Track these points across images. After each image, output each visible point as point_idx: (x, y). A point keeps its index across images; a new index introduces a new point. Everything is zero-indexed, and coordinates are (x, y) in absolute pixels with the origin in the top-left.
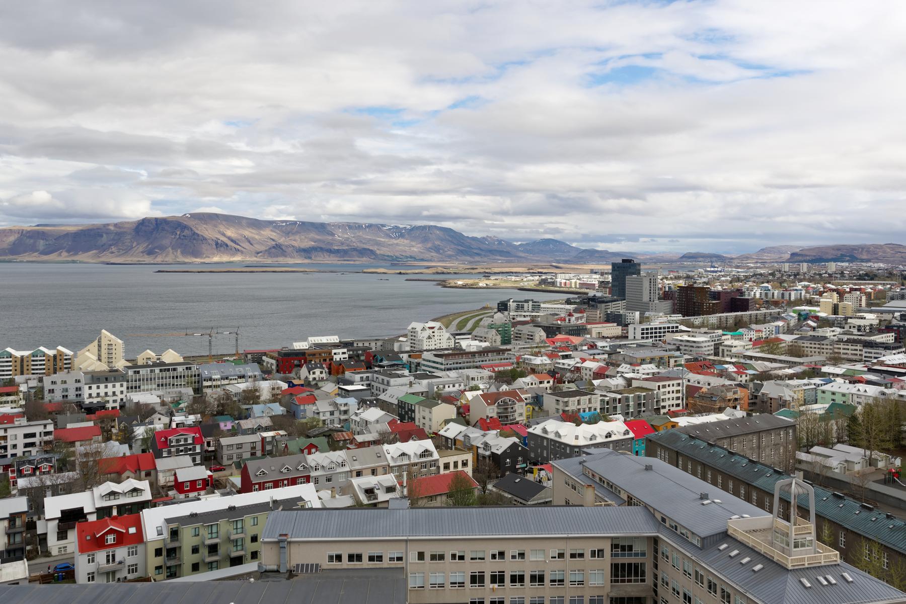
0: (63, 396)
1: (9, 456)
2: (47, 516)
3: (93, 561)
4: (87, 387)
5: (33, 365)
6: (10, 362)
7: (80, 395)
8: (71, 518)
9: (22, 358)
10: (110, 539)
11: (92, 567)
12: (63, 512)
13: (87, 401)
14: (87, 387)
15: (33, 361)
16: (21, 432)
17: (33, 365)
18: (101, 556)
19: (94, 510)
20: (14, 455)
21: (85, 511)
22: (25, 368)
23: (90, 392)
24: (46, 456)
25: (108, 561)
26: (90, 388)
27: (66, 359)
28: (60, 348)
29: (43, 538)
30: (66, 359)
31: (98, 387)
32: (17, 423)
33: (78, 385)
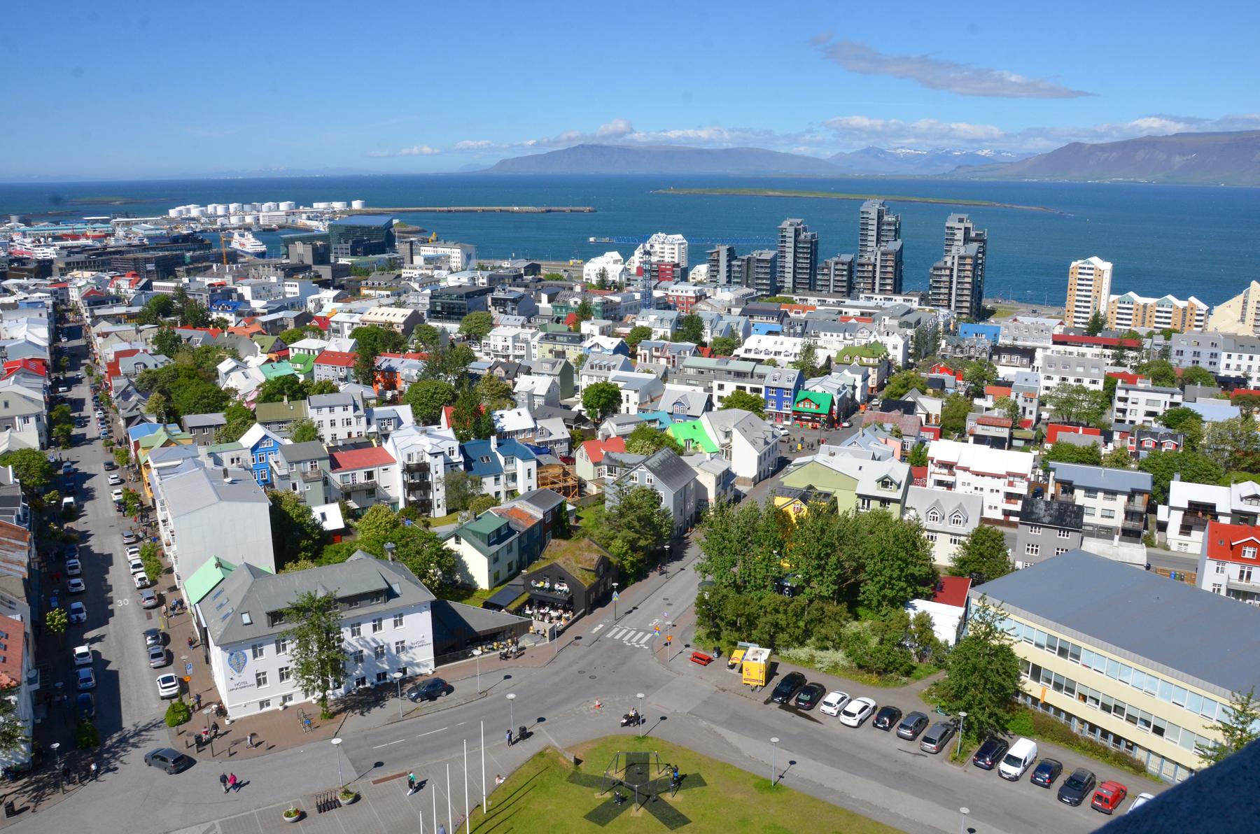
0: (1193, 362)
1: (1127, 422)
2: (1172, 502)
3: (1222, 572)
4: (1224, 355)
5: (1157, 317)
6: (1131, 309)
7: (1215, 364)
8: (1198, 514)
9: (1145, 306)
10: (1249, 553)
11: (1221, 579)
12: (1191, 503)
13: (1223, 373)
14: (1224, 355)
15: (1158, 311)
16: (1143, 397)
17: (1157, 317)
18: (1233, 569)
19: (1229, 512)
20: (1132, 422)
21: (1218, 510)
22: (1147, 319)
23: (1228, 361)
24: (1170, 431)
25: (1241, 577)
26: (1229, 356)
27: (1198, 315)
28: (1192, 299)
29: (1163, 527)
30: (1198, 315)
31: (1240, 357)
32: (1140, 385)
33: (1214, 350)
